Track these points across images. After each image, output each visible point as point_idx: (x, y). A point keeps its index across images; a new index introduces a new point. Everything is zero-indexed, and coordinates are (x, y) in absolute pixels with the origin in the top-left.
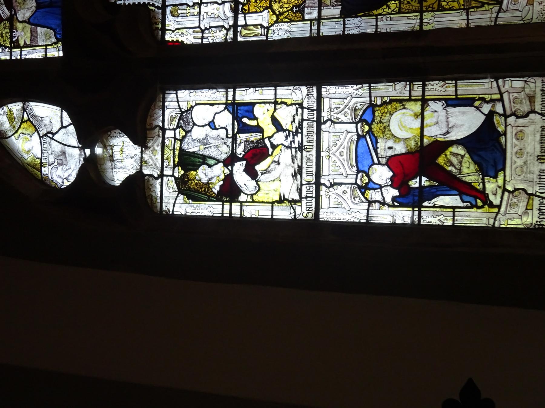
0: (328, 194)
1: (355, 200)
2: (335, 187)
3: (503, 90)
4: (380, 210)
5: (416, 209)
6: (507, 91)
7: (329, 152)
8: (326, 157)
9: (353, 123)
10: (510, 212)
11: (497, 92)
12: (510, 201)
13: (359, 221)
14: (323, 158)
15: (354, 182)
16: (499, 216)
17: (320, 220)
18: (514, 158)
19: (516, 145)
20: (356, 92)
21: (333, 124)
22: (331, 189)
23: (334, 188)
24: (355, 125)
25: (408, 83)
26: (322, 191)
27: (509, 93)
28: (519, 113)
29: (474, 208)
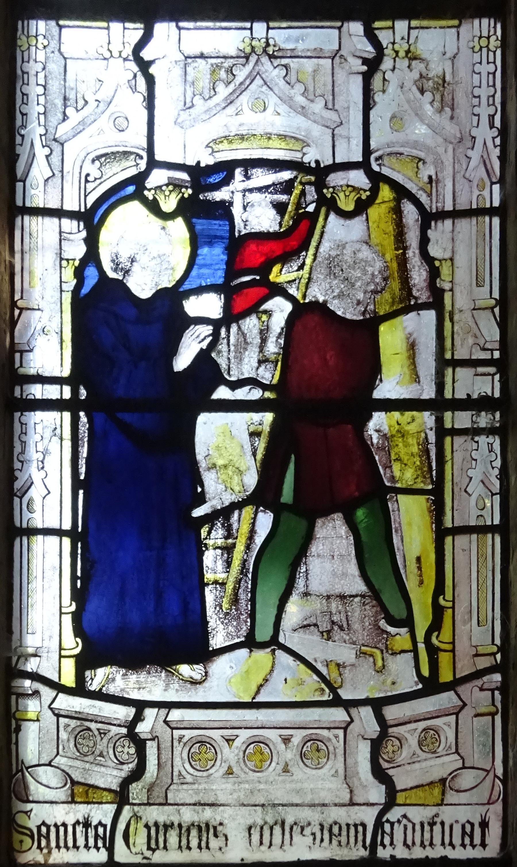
0: (116, 54)
1: (93, 161)
2: (142, 83)
3: (464, 690)
4: (61, 259)
5: (67, 393)
6: (465, 705)
7: (265, 51)
8: (247, 41)
9: (367, 151)
10: (61, 729)
11: (462, 672)
12: (100, 726)
13: (19, 175)
14: (245, 29)
15: (159, 157)
16: (47, 693)
17: (20, 23)
18: (244, 735)
19: (286, 740)
20: (475, 155)
21: (365, 68)
22: (134, 67)
23: (135, 76)
24: (358, 157)
25: (497, 355)
26: (125, 28)
27: (457, 714)
28: (389, 747)
29: (74, 604)
